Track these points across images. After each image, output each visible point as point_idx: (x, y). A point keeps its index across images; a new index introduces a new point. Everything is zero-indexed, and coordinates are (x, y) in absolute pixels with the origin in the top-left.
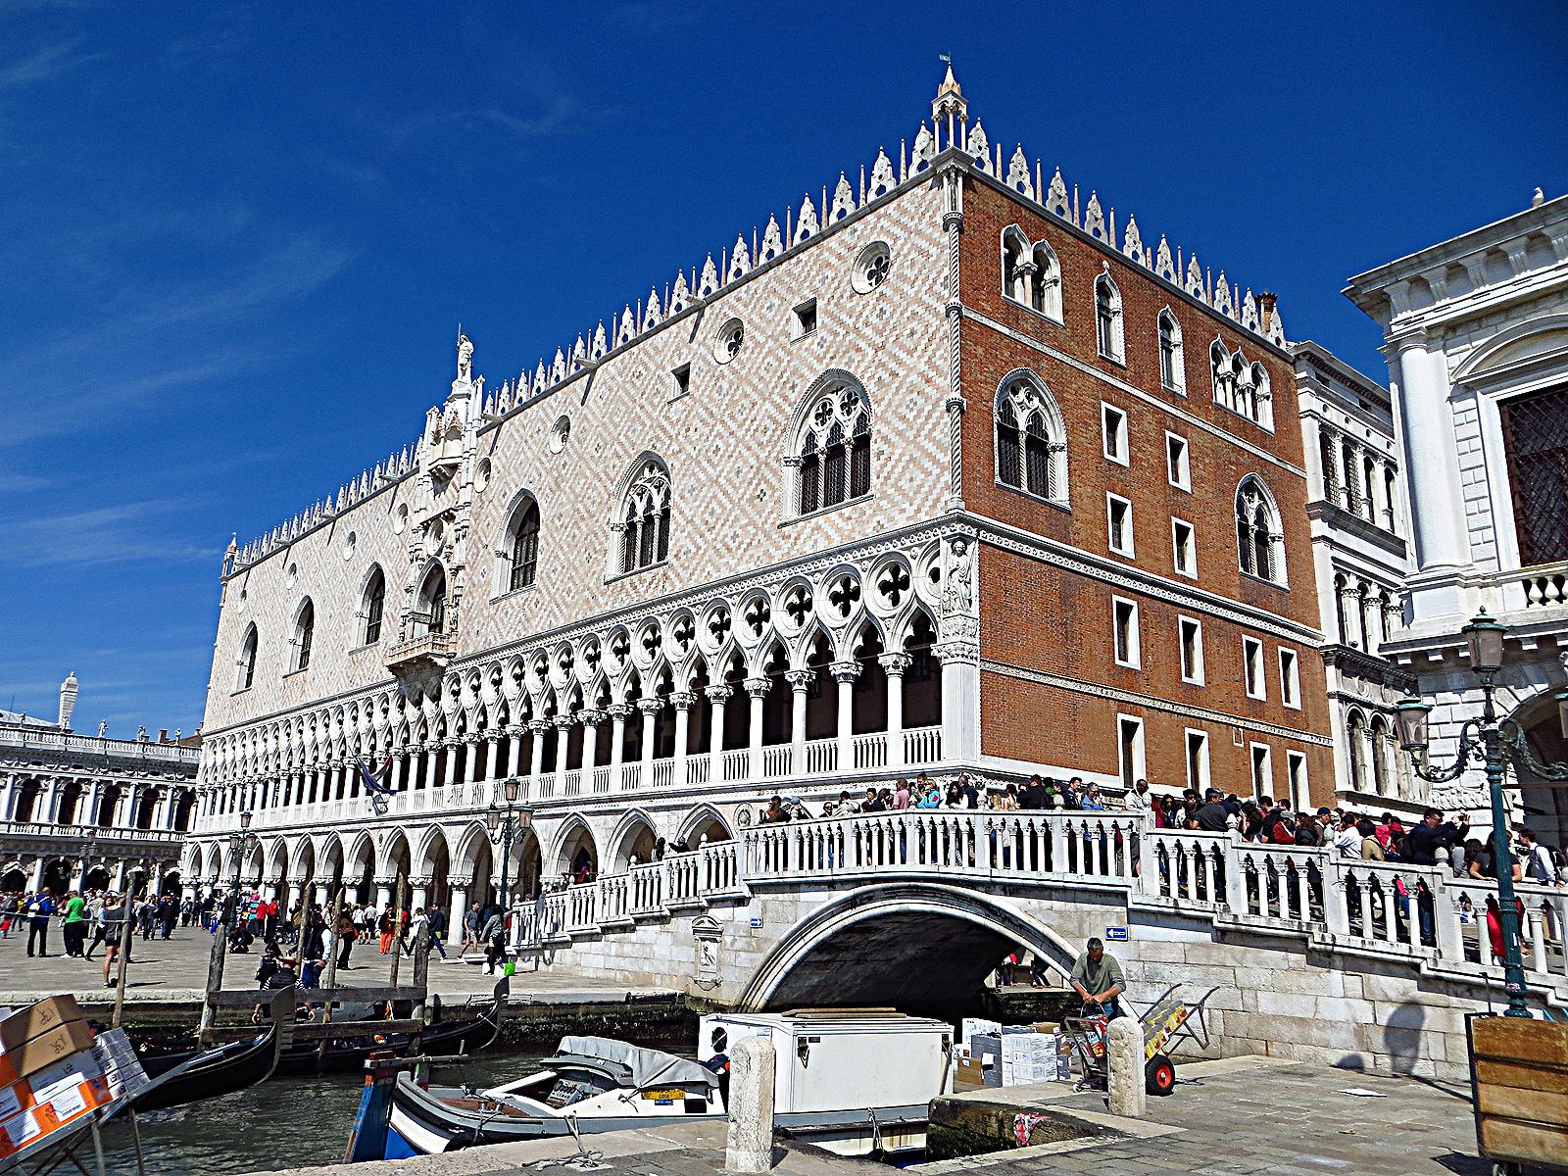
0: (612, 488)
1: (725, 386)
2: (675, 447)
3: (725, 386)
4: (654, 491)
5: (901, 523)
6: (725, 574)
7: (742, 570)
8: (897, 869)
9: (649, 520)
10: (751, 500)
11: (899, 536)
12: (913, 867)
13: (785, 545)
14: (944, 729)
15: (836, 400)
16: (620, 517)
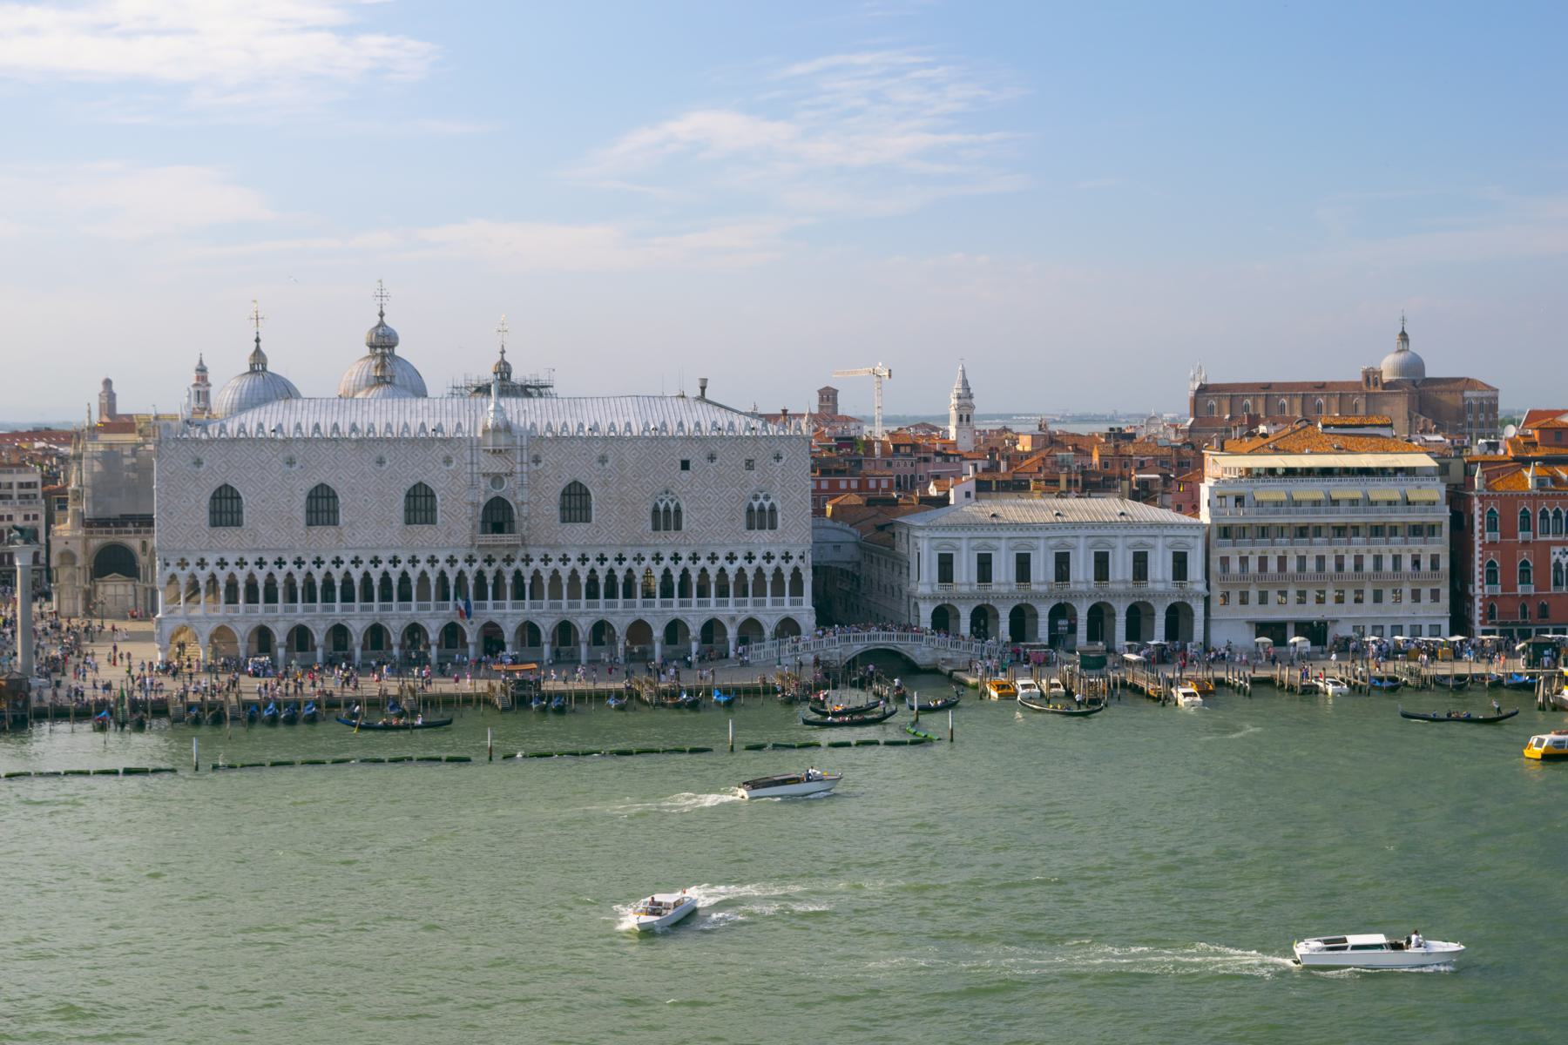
0: (647, 496)
1: (712, 476)
2: (685, 490)
3: (712, 476)
4: (670, 503)
5: (792, 541)
6: (717, 541)
7: (726, 542)
8: (877, 642)
9: (667, 510)
10: (729, 520)
11: (792, 545)
12: (881, 641)
13: (746, 539)
14: (804, 598)
15: (761, 495)
16: (651, 507)
